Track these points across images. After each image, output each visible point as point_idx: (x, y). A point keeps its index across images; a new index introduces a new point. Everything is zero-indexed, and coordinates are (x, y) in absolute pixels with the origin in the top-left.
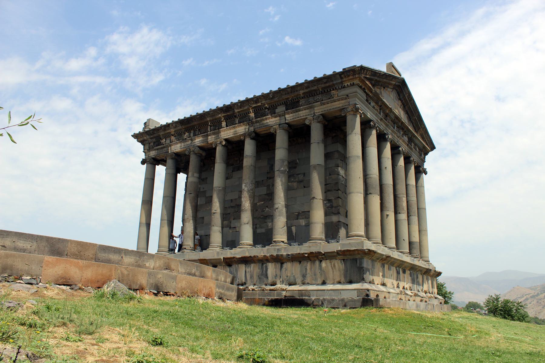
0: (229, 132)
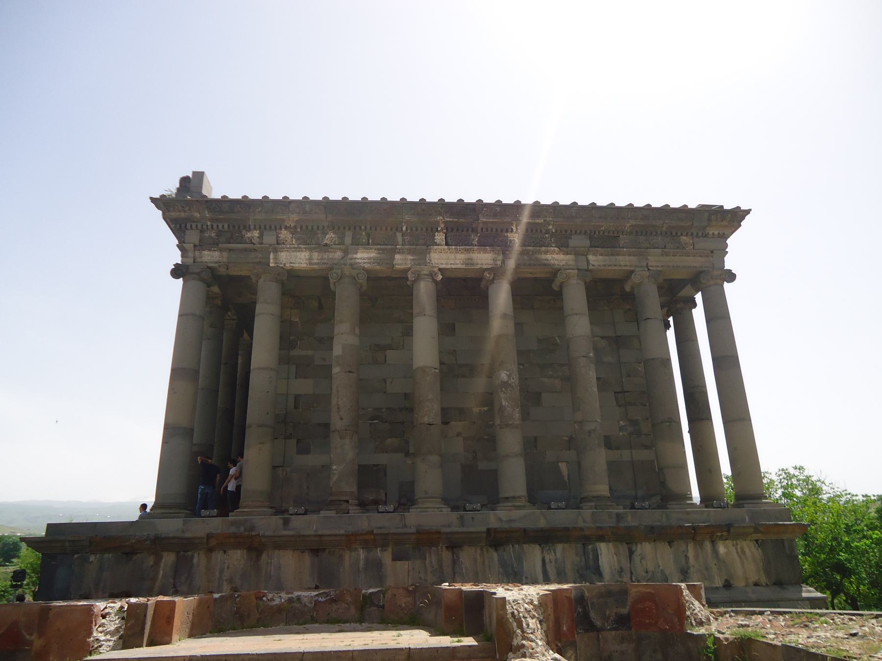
0: (452, 256)
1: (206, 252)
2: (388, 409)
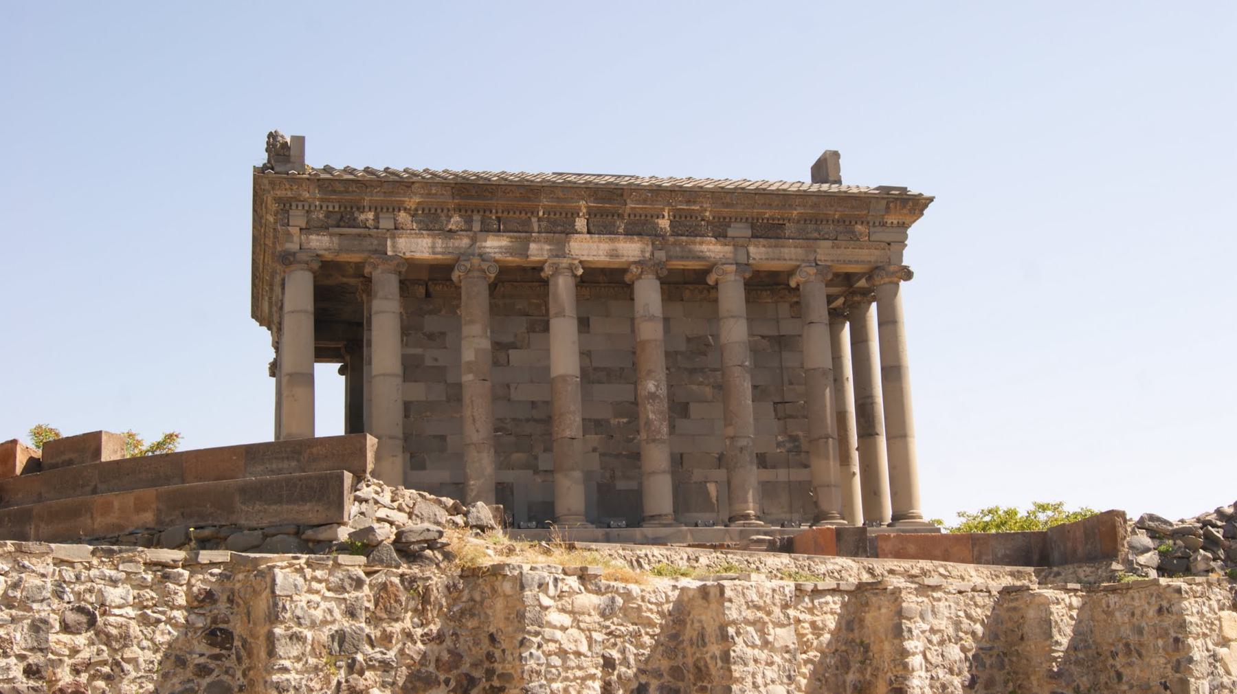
0: (594, 246)
1: (313, 237)
2: (514, 419)
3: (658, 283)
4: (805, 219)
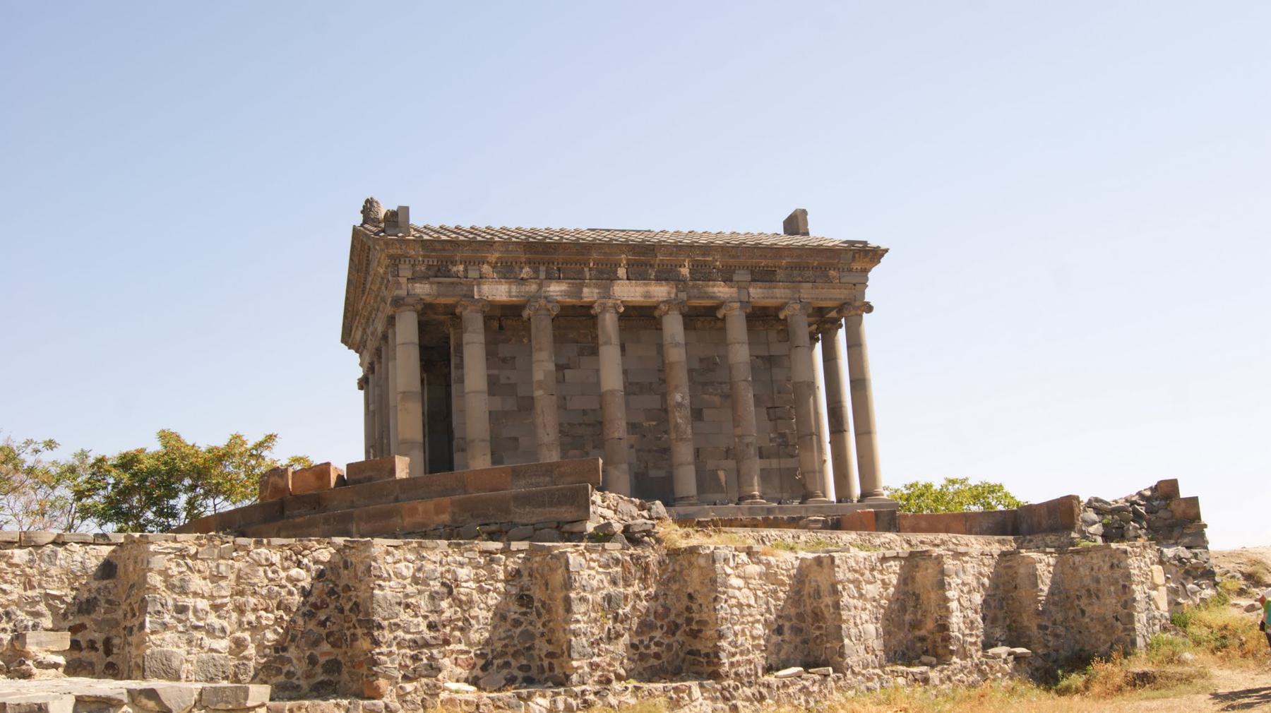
0: (632, 289)
3: (680, 318)
4: (792, 267)
